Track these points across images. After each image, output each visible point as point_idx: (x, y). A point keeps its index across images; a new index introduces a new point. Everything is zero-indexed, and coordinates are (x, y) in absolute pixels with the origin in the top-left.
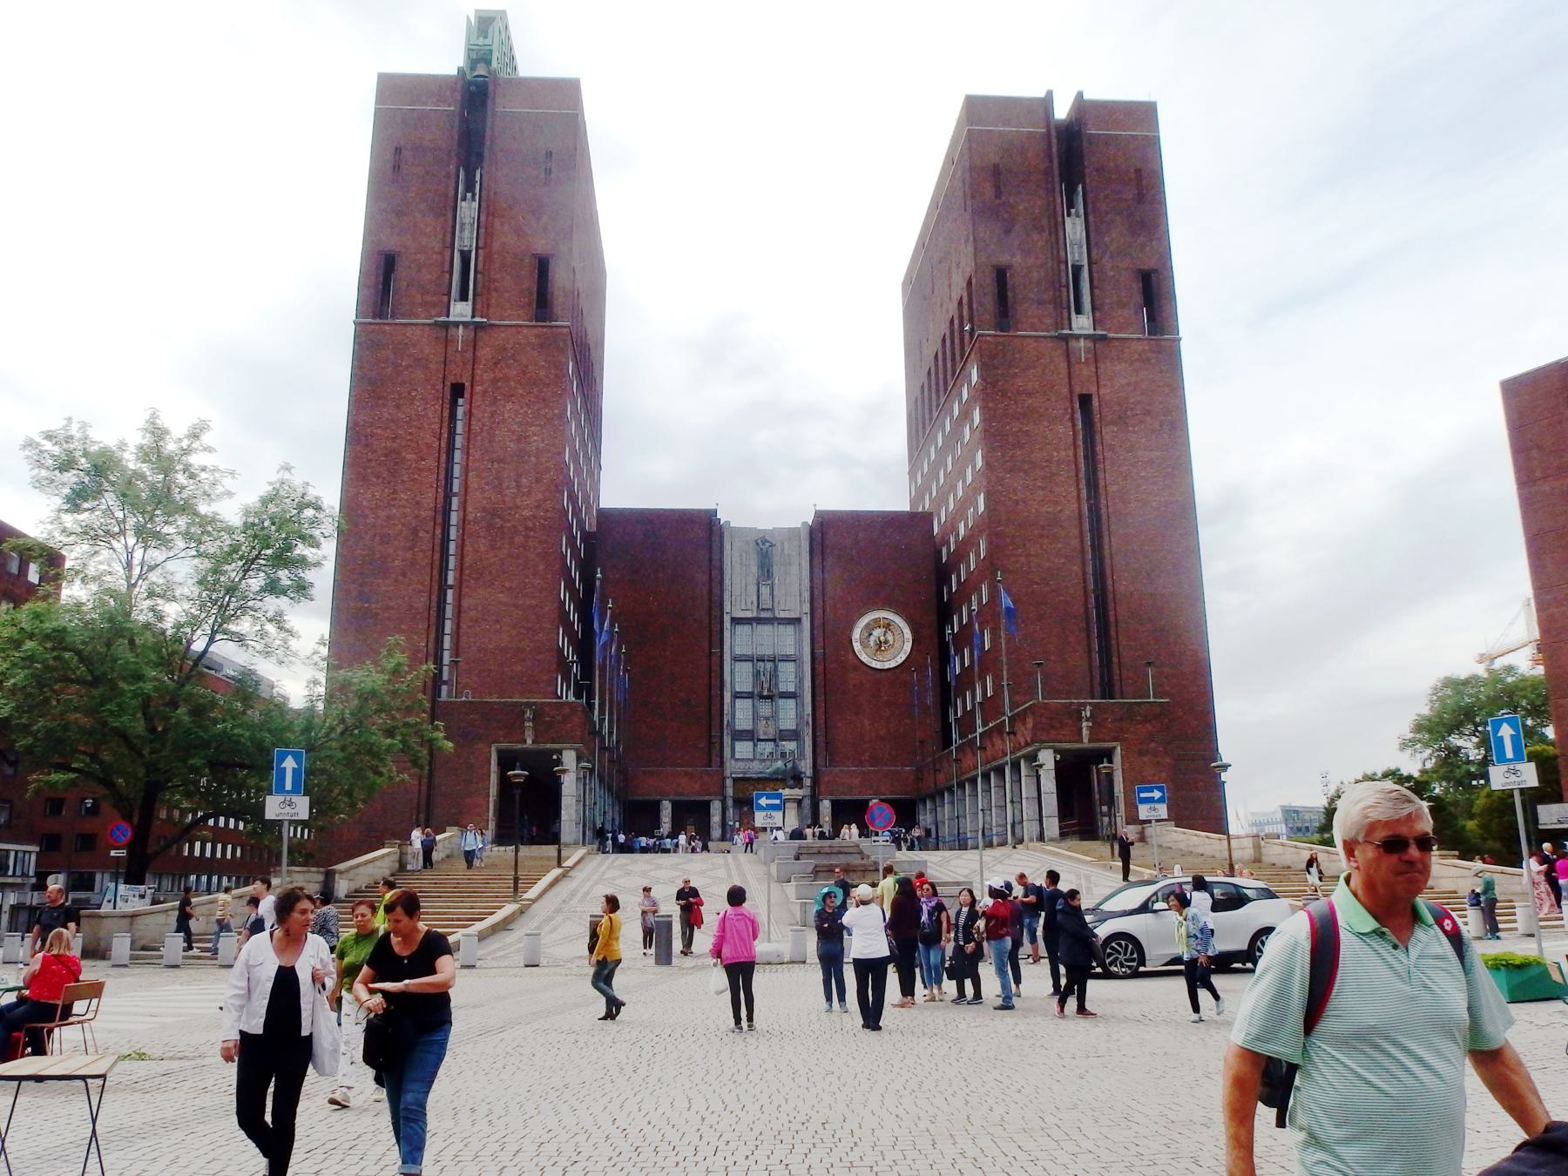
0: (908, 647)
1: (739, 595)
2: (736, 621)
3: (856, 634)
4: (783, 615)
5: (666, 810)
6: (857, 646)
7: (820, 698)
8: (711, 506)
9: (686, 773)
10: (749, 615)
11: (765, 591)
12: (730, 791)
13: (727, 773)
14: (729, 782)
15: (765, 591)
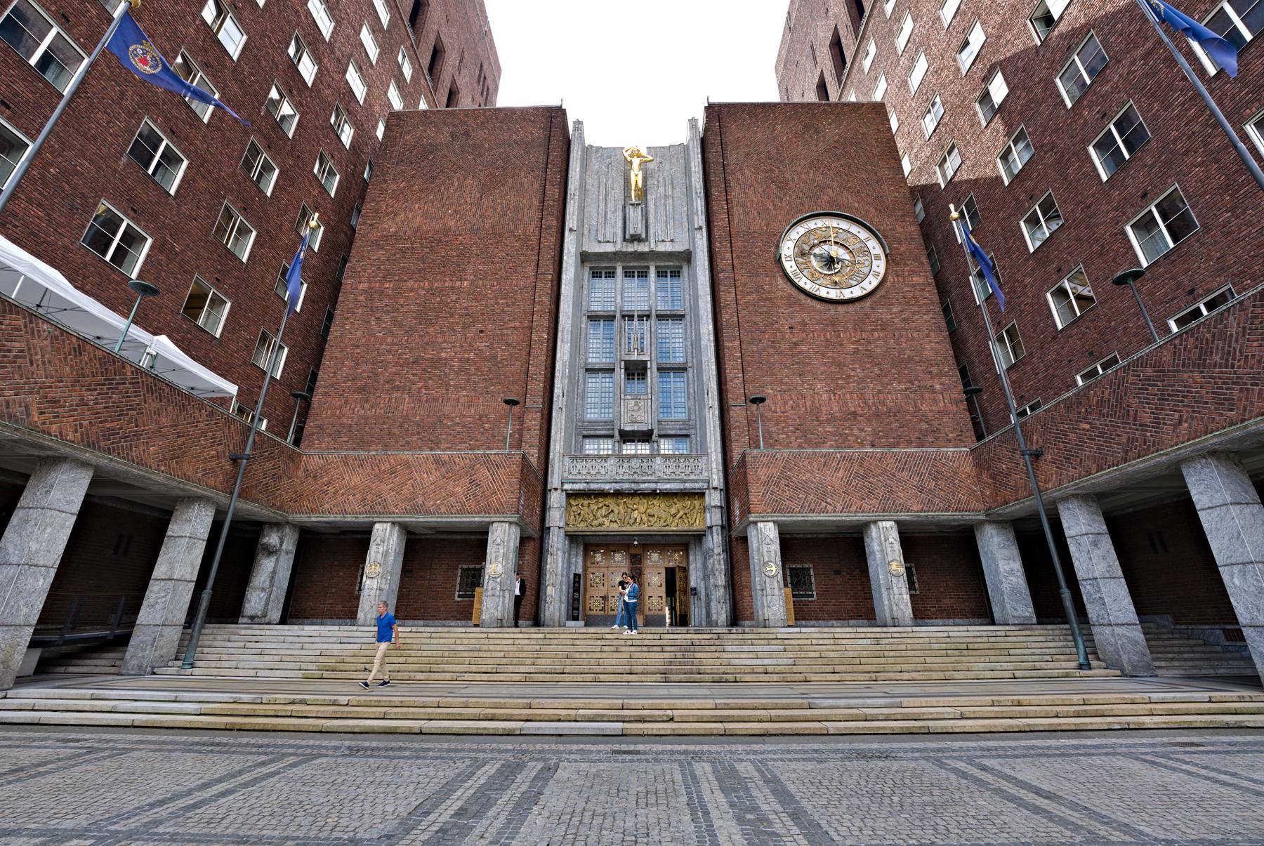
0: (880, 266)
1: (593, 224)
2: (584, 257)
3: (788, 249)
4: (662, 248)
5: (385, 546)
6: (790, 266)
7: (730, 344)
8: (558, 103)
9: (438, 462)
10: (609, 248)
11: (635, 215)
12: (556, 517)
13: (554, 481)
14: (556, 499)
15: (635, 215)
